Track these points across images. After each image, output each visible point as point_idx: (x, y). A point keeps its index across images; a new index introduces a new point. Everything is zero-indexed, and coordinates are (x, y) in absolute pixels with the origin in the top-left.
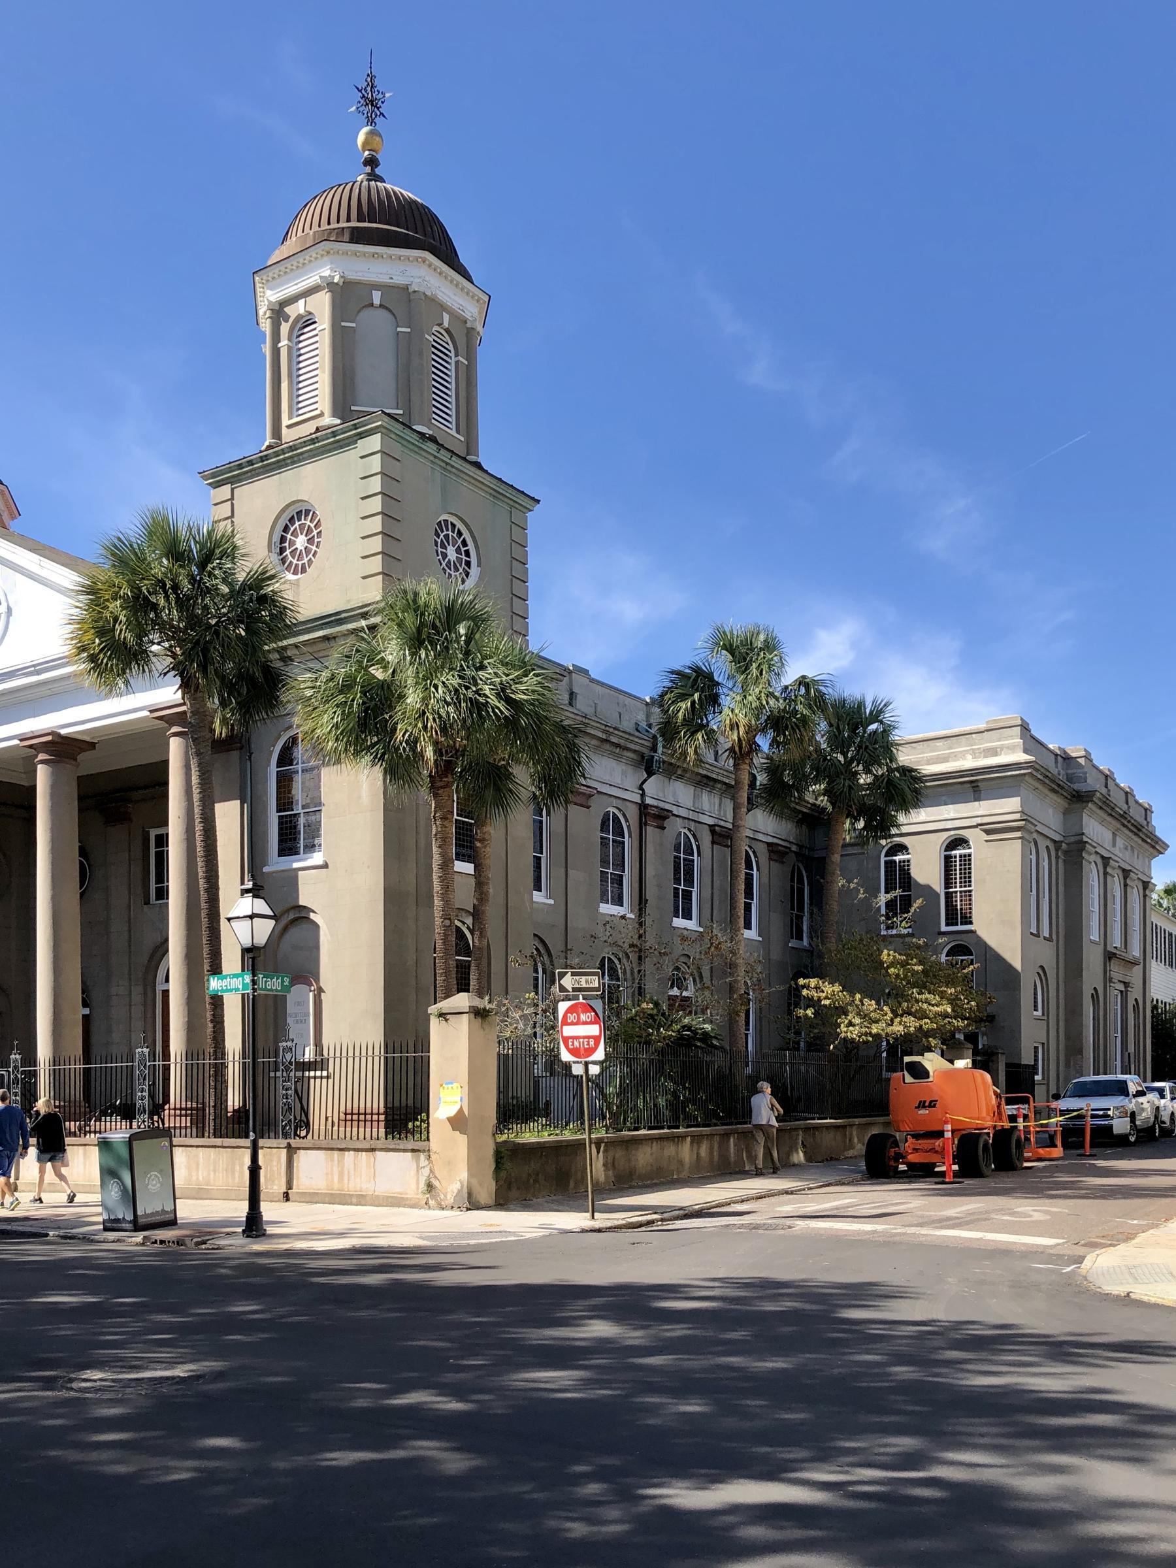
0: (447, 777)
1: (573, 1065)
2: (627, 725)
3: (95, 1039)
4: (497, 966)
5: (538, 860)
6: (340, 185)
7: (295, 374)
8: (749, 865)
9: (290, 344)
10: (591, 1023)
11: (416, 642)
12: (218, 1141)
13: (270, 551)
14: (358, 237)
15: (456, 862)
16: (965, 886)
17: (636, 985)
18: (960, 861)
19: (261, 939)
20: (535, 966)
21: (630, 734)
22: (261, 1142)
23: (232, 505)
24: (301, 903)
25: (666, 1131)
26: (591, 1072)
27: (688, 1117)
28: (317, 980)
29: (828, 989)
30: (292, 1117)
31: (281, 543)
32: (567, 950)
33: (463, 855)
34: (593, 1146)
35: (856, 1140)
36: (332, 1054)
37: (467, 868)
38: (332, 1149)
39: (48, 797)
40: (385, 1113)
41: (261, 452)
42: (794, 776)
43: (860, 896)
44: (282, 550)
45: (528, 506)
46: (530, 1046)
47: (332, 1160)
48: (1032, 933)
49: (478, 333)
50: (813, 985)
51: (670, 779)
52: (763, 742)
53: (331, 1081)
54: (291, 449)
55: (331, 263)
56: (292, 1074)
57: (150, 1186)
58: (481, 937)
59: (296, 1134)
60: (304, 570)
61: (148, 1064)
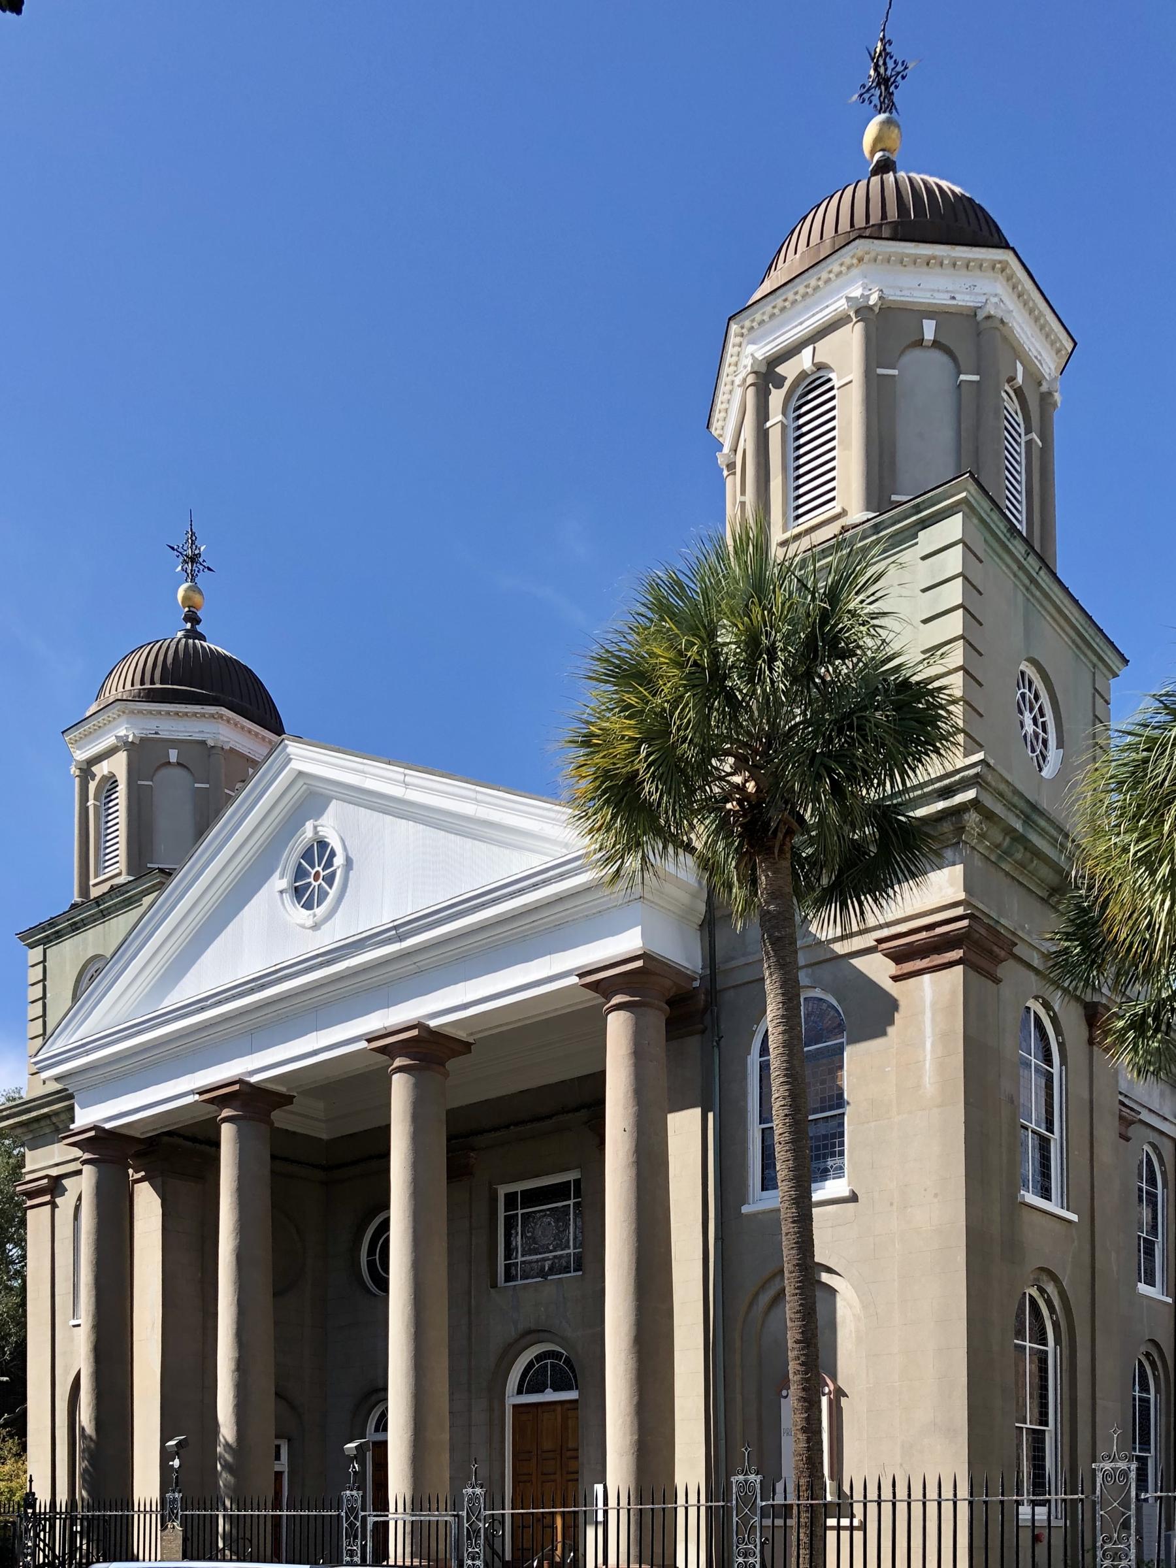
9: (785, 421)
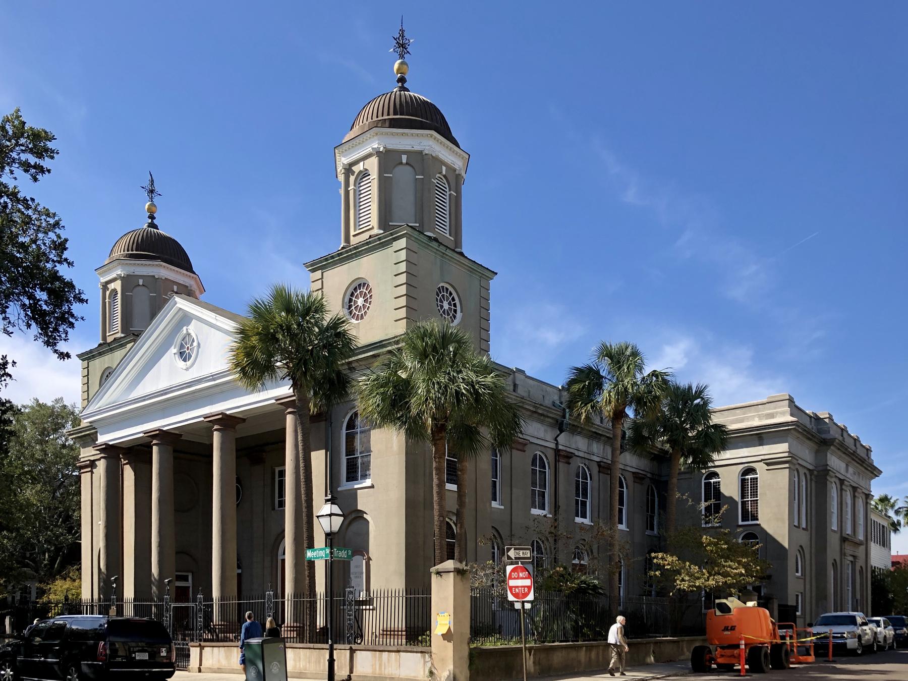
0: (441, 433)
1: (515, 603)
2: (548, 402)
3: (244, 587)
4: (470, 545)
5: (495, 483)
6: (384, 95)
7: (358, 205)
8: (621, 486)
9: (355, 188)
10: (526, 578)
11: (423, 356)
12: (311, 645)
13: (343, 307)
14: (394, 124)
15: (446, 484)
16: (754, 498)
17: (553, 556)
18: (751, 482)
19: (336, 528)
20: (493, 544)
21: (549, 408)
22: (335, 646)
23: (322, 282)
24: (359, 508)
25: (571, 643)
26: (525, 608)
27: (584, 635)
28: (368, 553)
29: (670, 559)
30: (353, 632)
31: (349, 303)
32: (512, 535)
33: (451, 480)
34: (527, 652)
35: (685, 650)
36: (375, 595)
37: (454, 487)
38: (375, 651)
39: (219, 450)
40: (406, 631)
41: (338, 251)
42: (650, 433)
43: (689, 503)
44: (350, 307)
45: (490, 276)
46: (490, 592)
47: (375, 657)
48: (795, 526)
49: (463, 177)
50: (660, 557)
51: (573, 434)
52: (630, 412)
53: (375, 612)
54: (355, 248)
55: (379, 140)
56: (353, 607)
57: (273, 670)
58: (461, 527)
59: (355, 642)
60: (362, 318)
61: (273, 601)
